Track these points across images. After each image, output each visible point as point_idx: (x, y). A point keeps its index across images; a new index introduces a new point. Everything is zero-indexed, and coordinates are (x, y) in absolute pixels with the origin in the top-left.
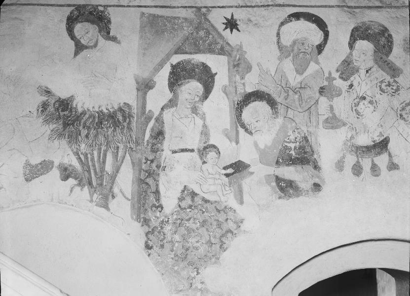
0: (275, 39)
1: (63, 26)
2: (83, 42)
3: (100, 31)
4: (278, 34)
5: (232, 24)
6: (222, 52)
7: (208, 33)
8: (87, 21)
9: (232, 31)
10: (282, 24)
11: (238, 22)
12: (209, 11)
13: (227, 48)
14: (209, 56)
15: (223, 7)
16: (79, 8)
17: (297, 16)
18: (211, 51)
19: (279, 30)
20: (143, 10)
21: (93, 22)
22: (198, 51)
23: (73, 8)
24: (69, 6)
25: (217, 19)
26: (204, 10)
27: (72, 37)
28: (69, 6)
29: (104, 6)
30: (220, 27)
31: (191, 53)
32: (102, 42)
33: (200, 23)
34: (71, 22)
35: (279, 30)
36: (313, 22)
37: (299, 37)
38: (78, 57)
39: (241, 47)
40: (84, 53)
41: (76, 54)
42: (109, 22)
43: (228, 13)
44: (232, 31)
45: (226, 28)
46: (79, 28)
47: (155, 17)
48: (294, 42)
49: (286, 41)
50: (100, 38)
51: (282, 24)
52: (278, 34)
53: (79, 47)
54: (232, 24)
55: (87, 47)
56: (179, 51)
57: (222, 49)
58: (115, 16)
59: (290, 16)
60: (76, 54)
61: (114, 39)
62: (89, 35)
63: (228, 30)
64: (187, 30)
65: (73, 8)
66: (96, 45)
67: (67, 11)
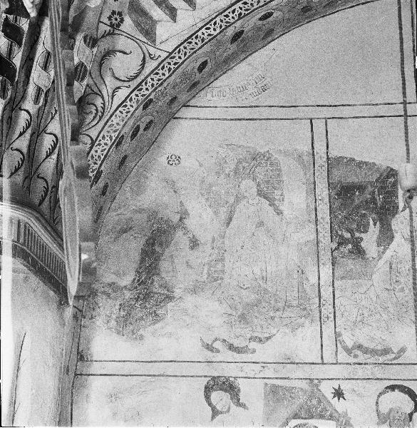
0: (374, 407)
1: (202, 393)
2: (219, 408)
3: (232, 399)
4: (377, 403)
5: (339, 394)
6: (331, 418)
7: (320, 402)
8: (221, 390)
9: (339, 399)
10: (379, 396)
11: (344, 392)
12: (320, 382)
13: (336, 415)
14: (320, 421)
15: (332, 379)
16: (214, 378)
17: (392, 388)
18: (322, 417)
19: (378, 400)
20: (265, 380)
21: (226, 391)
22: (312, 417)
23: (210, 379)
24: (205, 376)
25: (327, 389)
26: (316, 381)
27: (210, 404)
28: (205, 376)
29: (235, 378)
30: (329, 395)
31: (306, 419)
32: (233, 407)
33: (312, 392)
34: (208, 390)
35: (378, 400)
36: (405, 393)
37: (394, 406)
38: (215, 420)
39: (346, 414)
40: (219, 417)
41: (213, 417)
42: (239, 390)
43: (336, 384)
44: (339, 399)
45: (334, 397)
46: (215, 396)
47: (274, 385)
48: (391, 410)
49: (384, 408)
50: (232, 404)
51: (379, 396)
52: (377, 403)
53: (215, 413)
54: (339, 394)
55: (221, 413)
56: (296, 416)
57: (331, 416)
58: (242, 385)
59: (386, 388)
60: (213, 417)
61: (243, 406)
62: (223, 402)
63: (336, 398)
64: (302, 399)
65: (210, 379)
66: (228, 411)
67: (204, 381)
